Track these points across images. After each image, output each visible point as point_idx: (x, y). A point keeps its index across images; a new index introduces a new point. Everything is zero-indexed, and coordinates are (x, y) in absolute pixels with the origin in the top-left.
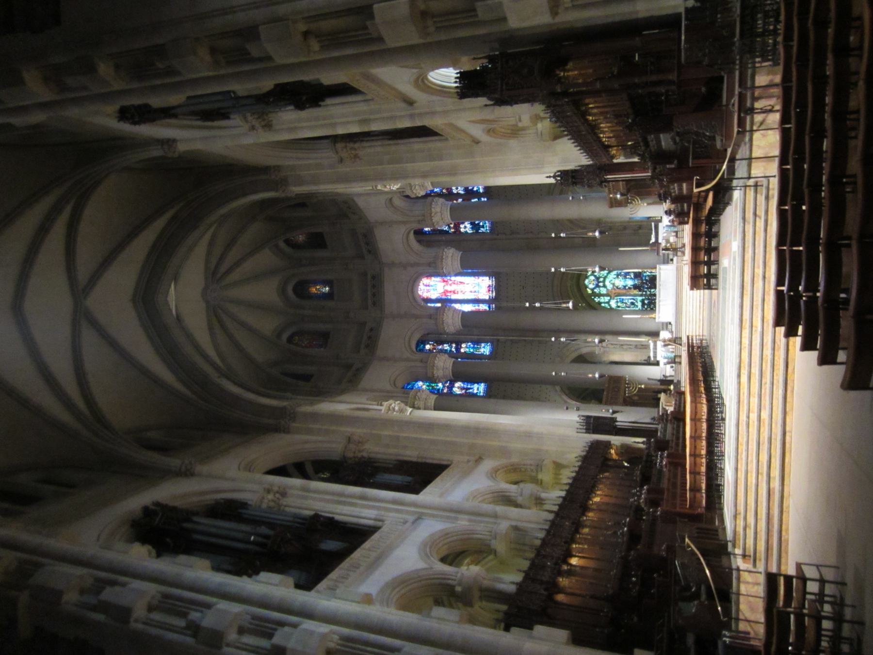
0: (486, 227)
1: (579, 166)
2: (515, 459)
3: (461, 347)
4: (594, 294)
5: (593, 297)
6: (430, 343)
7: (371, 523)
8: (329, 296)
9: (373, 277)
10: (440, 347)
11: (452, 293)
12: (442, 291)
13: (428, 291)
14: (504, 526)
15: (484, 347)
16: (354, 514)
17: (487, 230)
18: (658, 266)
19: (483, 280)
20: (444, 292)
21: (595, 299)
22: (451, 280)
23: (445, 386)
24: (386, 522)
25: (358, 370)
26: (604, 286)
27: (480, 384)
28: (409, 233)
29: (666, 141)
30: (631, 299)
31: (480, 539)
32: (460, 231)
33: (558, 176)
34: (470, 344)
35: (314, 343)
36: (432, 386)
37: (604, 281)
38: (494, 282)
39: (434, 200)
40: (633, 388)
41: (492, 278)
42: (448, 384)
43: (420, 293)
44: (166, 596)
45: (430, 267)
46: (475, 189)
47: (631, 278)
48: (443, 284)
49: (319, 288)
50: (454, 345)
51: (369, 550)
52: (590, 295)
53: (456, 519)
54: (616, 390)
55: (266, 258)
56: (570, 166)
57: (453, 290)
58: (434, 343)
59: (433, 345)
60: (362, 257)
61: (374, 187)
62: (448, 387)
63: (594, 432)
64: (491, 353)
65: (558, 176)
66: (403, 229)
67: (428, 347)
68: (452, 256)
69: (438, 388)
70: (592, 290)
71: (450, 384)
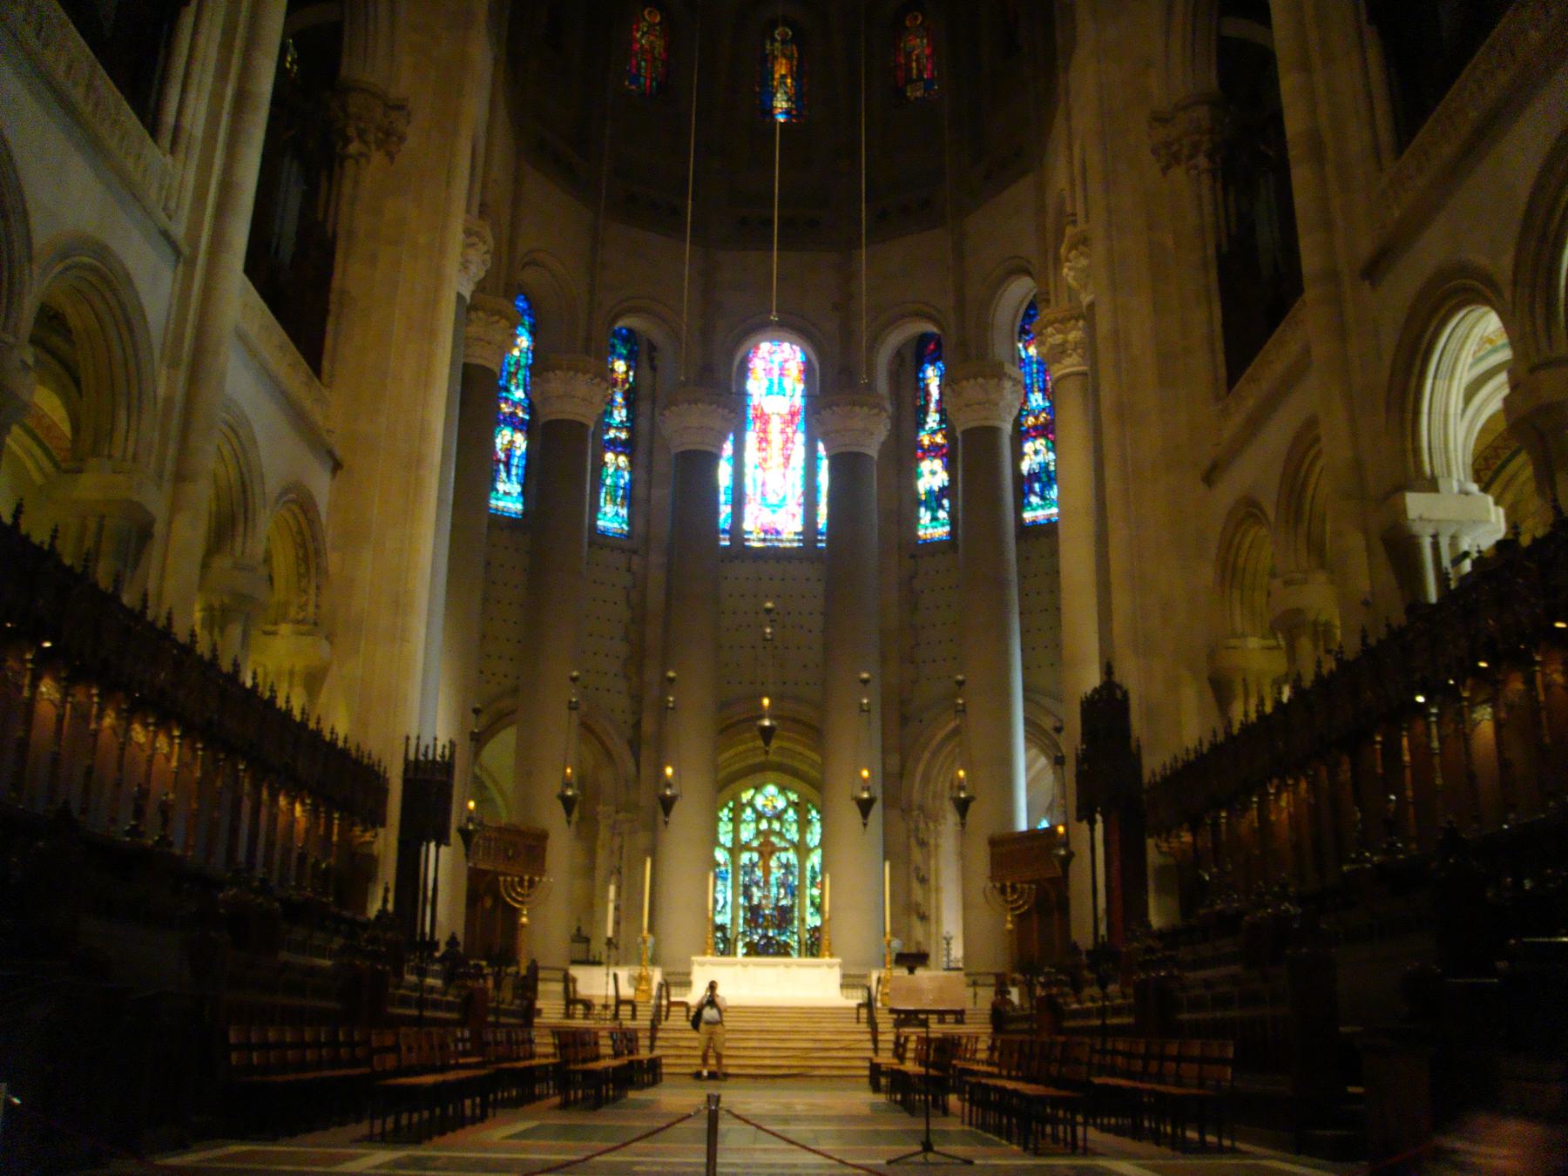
1: (1139, 746)
3: (617, 454)
4: (738, 809)
5: (731, 804)
6: (631, 373)
7: (169, 117)
10: (619, 399)
11: (761, 435)
12: (767, 410)
13: (768, 372)
14: (156, 502)
15: (617, 514)
16: (196, 68)
17: (926, 528)
18: (837, 960)
19: (794, 515)
20: (763, 414)
21: (726, 811)
22: (794, 432)
23: (516, 408)
24: (168, 156)
27: (521, 500)
28: (929, 318)
30: (725, 898)
31: (113, 429)
32: (923, 458)
34: (627, 476)
35: (643, 64)
36: (515, 374)
38: (788, 545)
39: (1016, 388)
40: (517, 893)
41: (799, 540)
42: (521, 414)
43: (765, 347)
46: (1034, 500)
47: (778, 900)
48: (785, 410)
49: (785, 84)
50: (623, 435)
51: (90, 86)
52: (736, 798)
53: (174, 365)
54: (510, 853)
57: (770, 437)
58: (630, 384)
59: (626, 380)
61: (1071, 218)
62: (513, 415)
63: (407, 782)
64: (604, 534)
67: (620, 366)
69: (513, 388)
70: (751, 804)
71: (522, 419)
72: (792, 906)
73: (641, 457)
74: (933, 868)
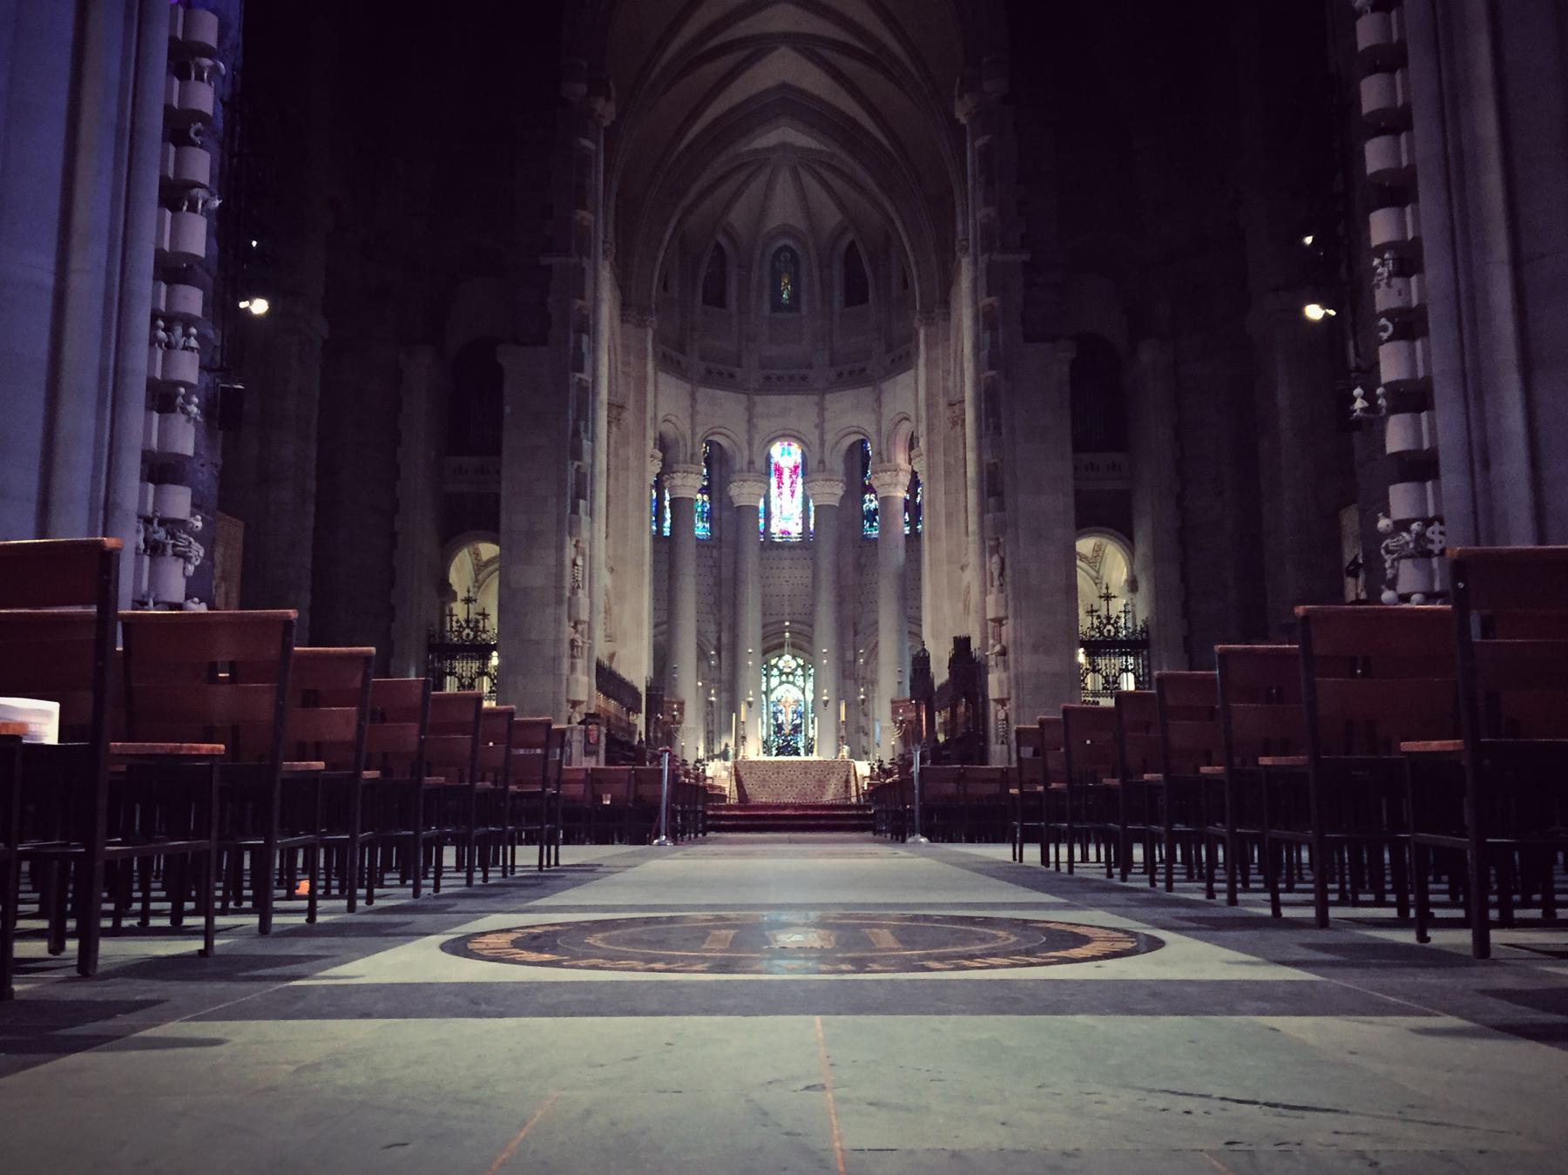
2: (615, 610)
8: (777, 305)
9: (804, 378)
12: (782, 465)
15: (704, 527)
19: (797, 524)
25: (679, 363)
26: (781, 683)
33: (924, 654)
34: (708, 506)
37: (788, 682)
38: (795, 540)
44: (587, 388)
45: (819, 463)
47: (793, 721)
48: (791, 465)
55: (831, 217)
57: (784, 481)
60: (832, 364)
63: (647, 695)
65: (924, 654)
66: (871, 430)
68: (832, 493)
70: (776, 666)
72: (801, 723)
73: (715, 495)
74: (871, 708)
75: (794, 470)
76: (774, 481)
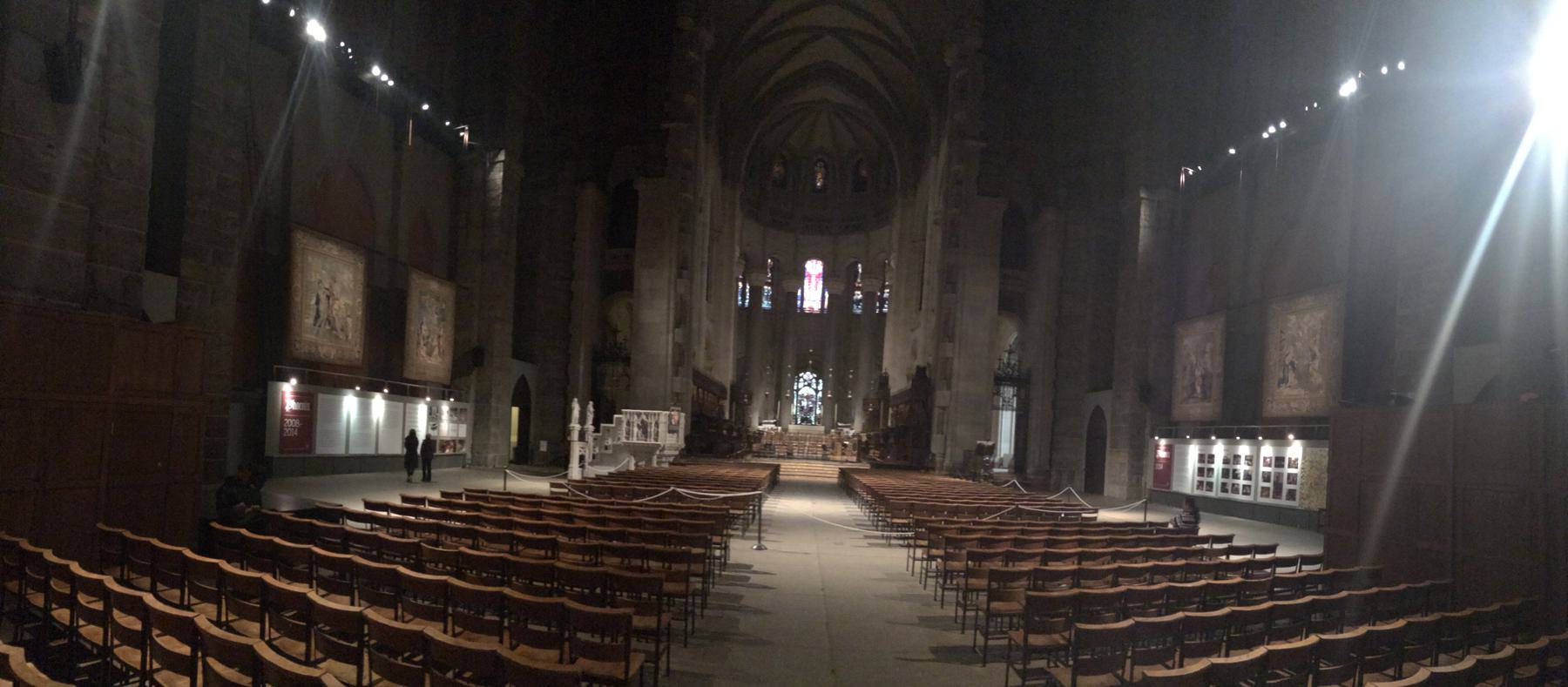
0: (858, 310)
4: (799, 378)
26: (805, 386)
29: (892, 440)
56: (891, 383)
70: (802, 377)
75: (818, 277)
76: (806, 281)
